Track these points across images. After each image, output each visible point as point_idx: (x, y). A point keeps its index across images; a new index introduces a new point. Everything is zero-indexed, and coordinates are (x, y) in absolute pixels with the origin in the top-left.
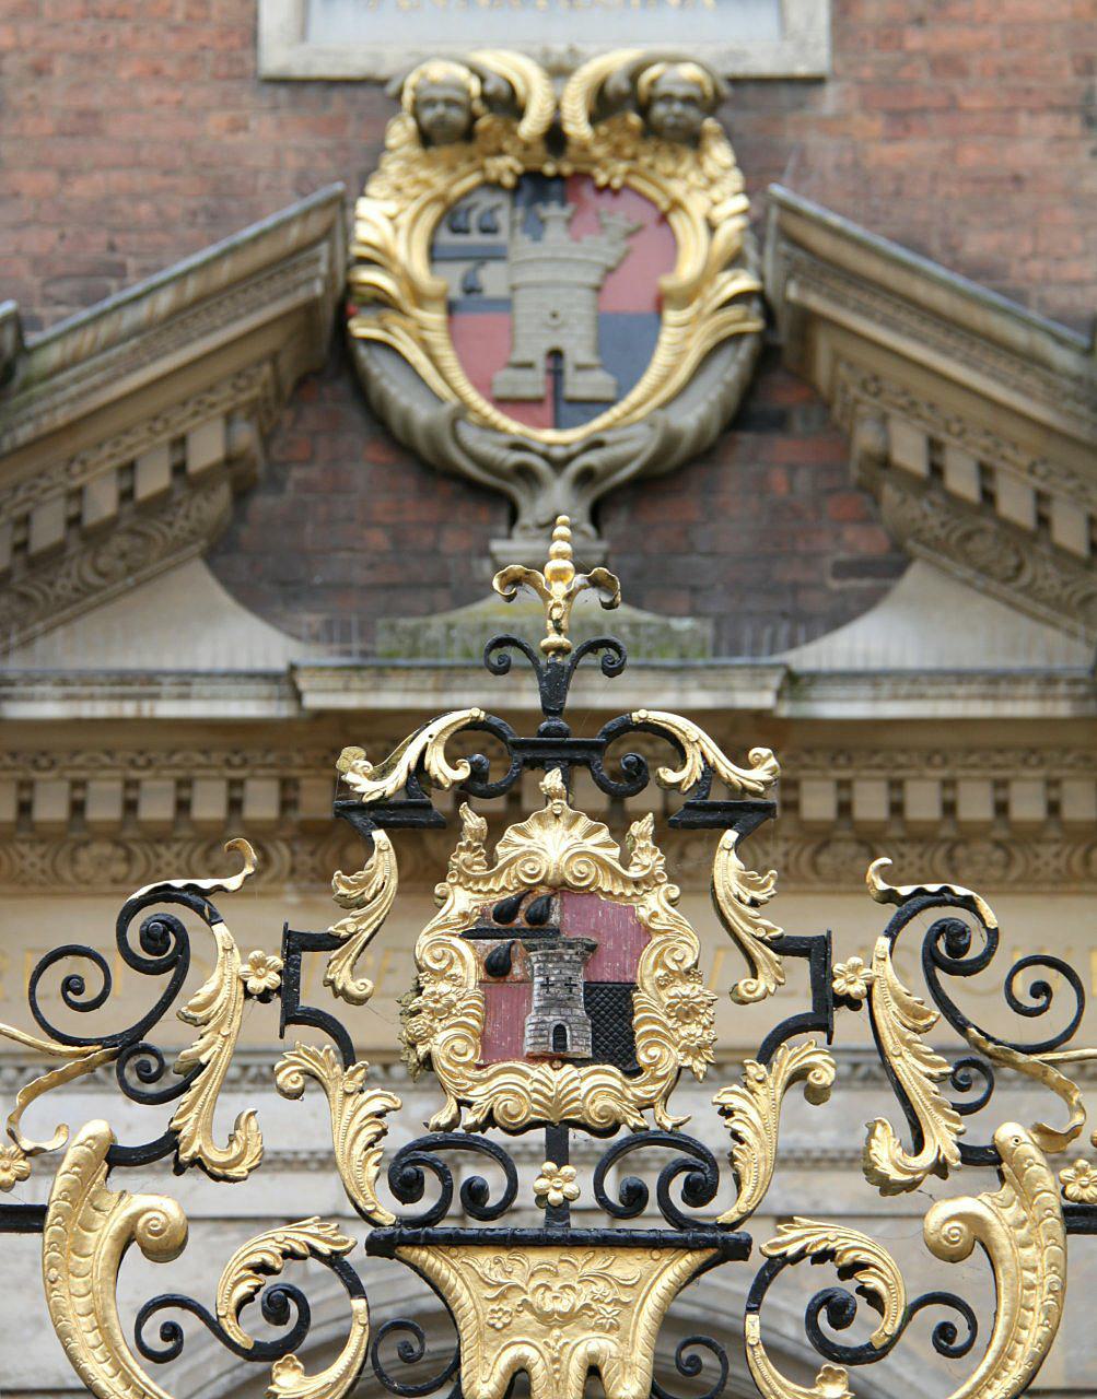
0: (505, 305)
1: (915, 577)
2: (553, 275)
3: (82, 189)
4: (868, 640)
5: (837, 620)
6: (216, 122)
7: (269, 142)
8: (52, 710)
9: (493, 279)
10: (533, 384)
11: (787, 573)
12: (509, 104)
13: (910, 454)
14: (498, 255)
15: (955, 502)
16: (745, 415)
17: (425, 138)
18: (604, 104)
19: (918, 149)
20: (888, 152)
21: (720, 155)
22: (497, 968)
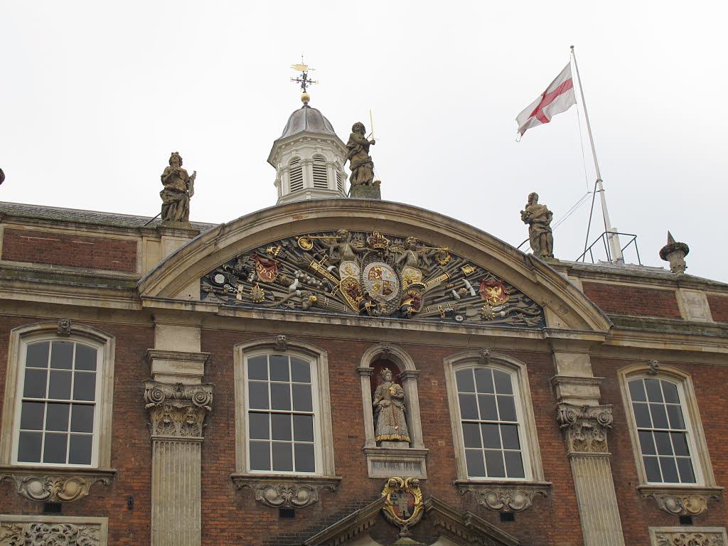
0: (398, 505)
1: (441, 537)
2: (403, 502)
3: (352, 490)
6: (364, 483)
7: (370, 485)
9: (396, 502)
10: (402, 515)
12: (399, 484)
13: (443, 524)
14: (397, 500)
15: (447, 530)
16: (423, 518)
17: (389, 486)
18: (408, 483)
19: (436, 488)
20: (433, 488)
21: (419, 489)
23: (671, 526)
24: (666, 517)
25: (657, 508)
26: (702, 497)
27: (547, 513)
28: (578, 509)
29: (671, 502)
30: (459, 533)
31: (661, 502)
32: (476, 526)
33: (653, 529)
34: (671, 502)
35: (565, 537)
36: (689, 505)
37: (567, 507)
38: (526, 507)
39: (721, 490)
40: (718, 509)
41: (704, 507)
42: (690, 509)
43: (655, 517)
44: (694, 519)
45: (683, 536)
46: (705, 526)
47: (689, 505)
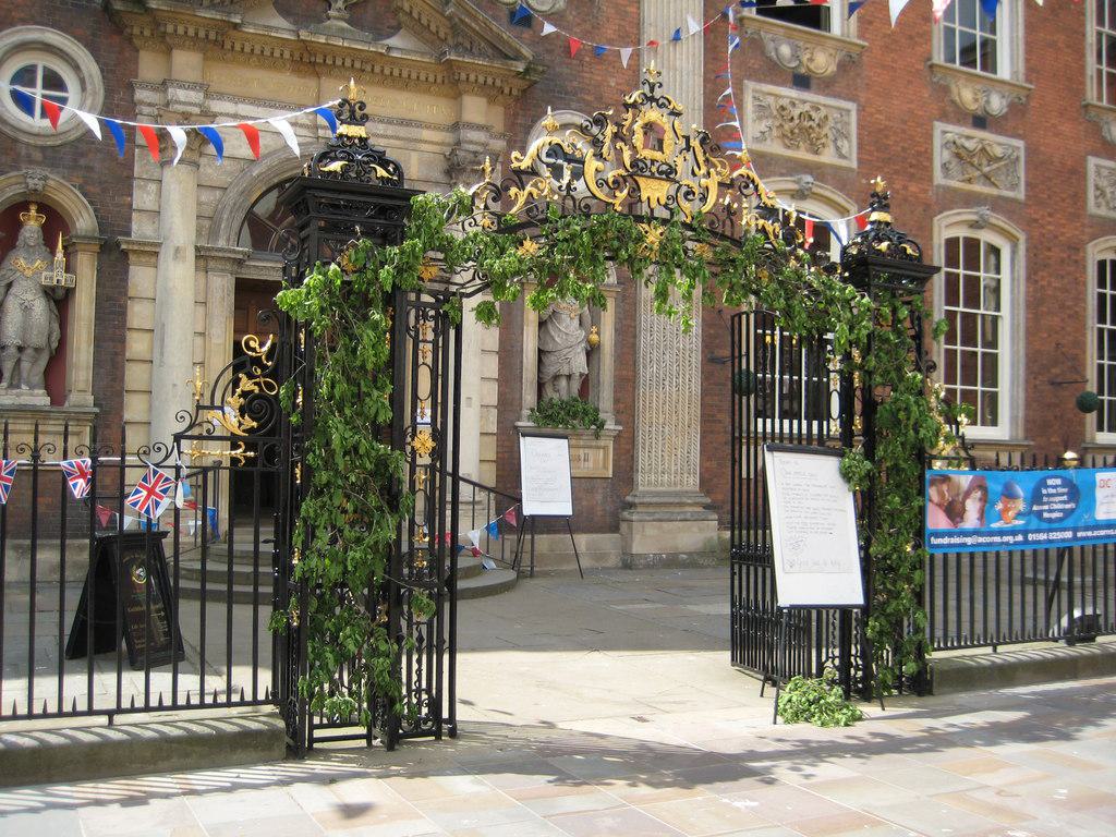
4: (393, 41)
5: (389, 37)
8: (251, 31)
11: (379, 26)
13: (406, 7)
22: (645, 133)
23: (777, 85)
24: (773, 71)
25: (763, 53)
26: (833, 52)
27: (588, 26)
28: (639, 29)
29: (785, 50)
30: (433, 28)
31: (771, 46)
32: (463, 17)
33: (750, 86)
34: (785, 50)
35: (611, 70)
36: (811, 60)
37: (623, 23)
38: (553, 11)
39: (863, 47)
40: (852, 74)
41: (832, 68)
42: (812, 66)
43: (756, 66)
44: (814, 82)
45: (794, 105)
46: (827, 95)
47: (811, 60)
